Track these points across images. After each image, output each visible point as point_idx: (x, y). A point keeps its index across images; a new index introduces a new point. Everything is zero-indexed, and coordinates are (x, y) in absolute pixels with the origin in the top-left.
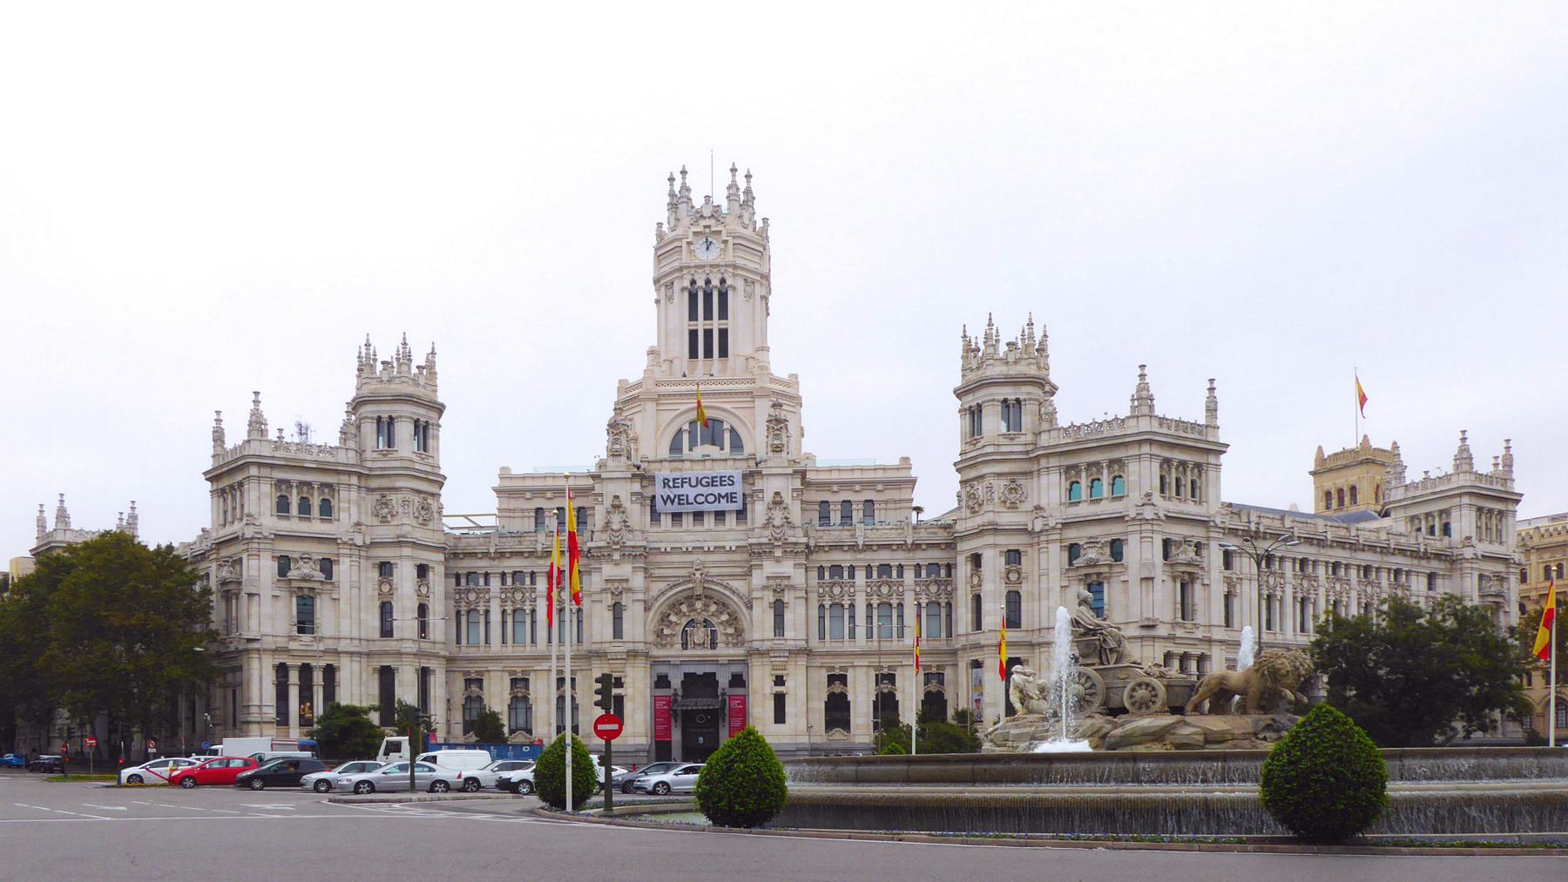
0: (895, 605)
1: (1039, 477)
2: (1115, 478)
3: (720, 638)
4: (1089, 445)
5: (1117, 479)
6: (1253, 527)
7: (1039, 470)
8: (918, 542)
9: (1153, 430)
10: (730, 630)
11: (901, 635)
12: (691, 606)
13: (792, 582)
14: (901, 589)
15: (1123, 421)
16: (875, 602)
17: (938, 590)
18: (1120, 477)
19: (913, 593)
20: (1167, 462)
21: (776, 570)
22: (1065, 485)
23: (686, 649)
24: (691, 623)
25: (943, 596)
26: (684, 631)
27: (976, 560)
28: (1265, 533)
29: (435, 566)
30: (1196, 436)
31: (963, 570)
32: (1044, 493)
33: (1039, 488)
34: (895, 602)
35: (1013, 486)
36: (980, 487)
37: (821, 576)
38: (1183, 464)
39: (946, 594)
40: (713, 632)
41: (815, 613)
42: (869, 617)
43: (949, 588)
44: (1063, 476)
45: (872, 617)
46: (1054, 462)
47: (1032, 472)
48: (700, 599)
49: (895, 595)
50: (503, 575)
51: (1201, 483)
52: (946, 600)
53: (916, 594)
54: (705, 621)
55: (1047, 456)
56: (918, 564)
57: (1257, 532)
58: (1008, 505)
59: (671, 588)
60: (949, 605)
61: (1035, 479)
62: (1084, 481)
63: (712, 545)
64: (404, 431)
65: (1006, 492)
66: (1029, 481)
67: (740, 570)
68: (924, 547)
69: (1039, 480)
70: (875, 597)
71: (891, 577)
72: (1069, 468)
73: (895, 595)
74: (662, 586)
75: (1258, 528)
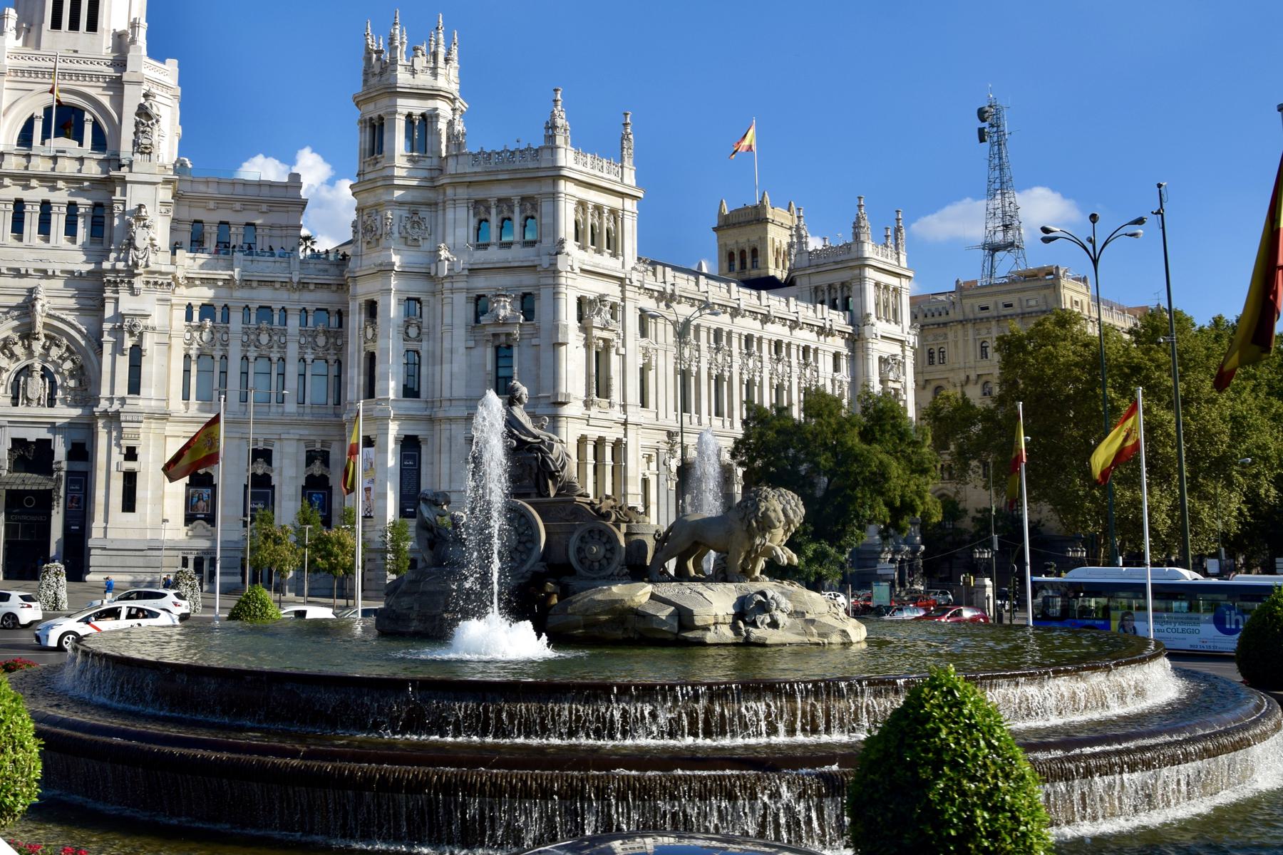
0: (275, 359)
1: (444, 210)
2: (527, 218)
3: (60, 394)
4: (500, 177)
5: (529, 220)
6: (669, 291)
7: (444, 202)
8: (305, 281)
9: (568, 165)
10: (72, 383)
11: (280, 400)
13: (149, 322)
14: (283, 340)
15: (537, 150)
16: (252, 354)
17: (327, 343)
18: (533, 218)
19: (297, 345)
20: (582, 204)
22: (473, 222)
23: (15, 404)
24: (27, 371)
25: (332, 351)
26: (17, 380)
27: (371, 309)
28: (681, 296)
30: (612, 177)
31: (356, 319)
32: (449, 231)
33: (444, 224)
34: (275, 356)
35: (416, 219)
36: (378, 218)
37: (189, 317)
38: (598, 208)
39: (335, 349)
40: (53, 382)
41: (178, 365)
42: (245, 374)
43: (339, 342)
44: (471, 212)
45: (247, 373)
46: (462, 192)
47: (436, 204)
48: (38, 339)
49: (275, 346)
52: (335, 357)
53: (300, 348)
54: (43, 368)
55: (454, 185)
56: (304, 309)
57: (673, 295)
58: (409, 242)
60: (339, 362)
61: (440, 213)
62: (494, 219)
65: (408, 226)
66: (433, 214)
67: (91, 302)
68: (312, 287)
69: (444, 214)
70: (252, 348)
71: (272, 323)
72: (477, 202)
73: (275, 346)
75: (673, 291)
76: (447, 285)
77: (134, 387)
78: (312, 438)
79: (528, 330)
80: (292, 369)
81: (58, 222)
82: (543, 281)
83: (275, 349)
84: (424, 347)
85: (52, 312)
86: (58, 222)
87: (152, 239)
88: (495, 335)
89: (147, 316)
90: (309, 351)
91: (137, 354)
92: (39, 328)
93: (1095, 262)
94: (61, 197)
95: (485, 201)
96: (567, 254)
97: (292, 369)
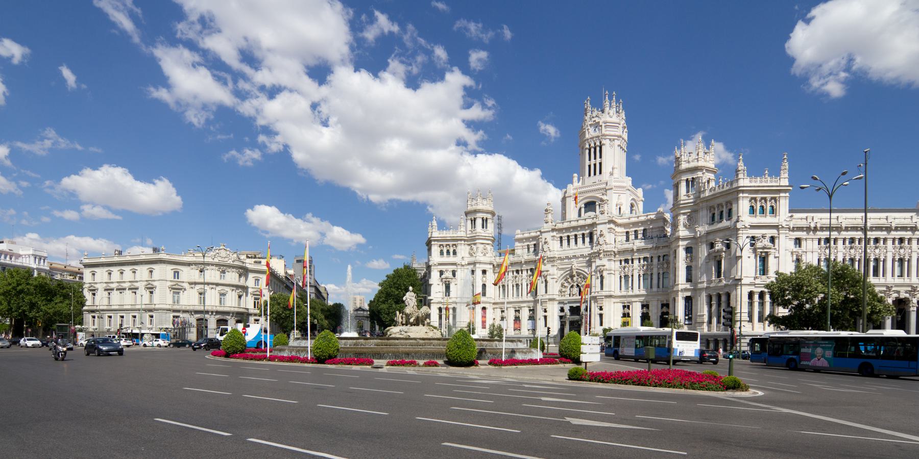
12: (572, 279)
19: (657, 268)
21: (601, 263)
29: (489, 270)
50: (513, 271)
51: (776, 207)
53: (658, 269)
59: (564, 273)
63: (579, 254)
64: (479, 222)
74: (562, 272)
75: (816, 225)
76: (700, 240)
77: (602, 288)
78: (662, 299)
79: (728, 252)
80: (655, 277)
81: (580, 240)
82: (733, 233)
83: (649, 270)
84: (693, 264)
85: (578, 268)
86: (580, 240)
87: (605, 241)
88: (716, 257)
89: (604, 266)
90: (661, 270)
91: (602, 277)
92: (574, 273)
93: (830, 197)
94: (579, 233)
95: (713, 206)
96: (742, 221)
97: (655, 277)
